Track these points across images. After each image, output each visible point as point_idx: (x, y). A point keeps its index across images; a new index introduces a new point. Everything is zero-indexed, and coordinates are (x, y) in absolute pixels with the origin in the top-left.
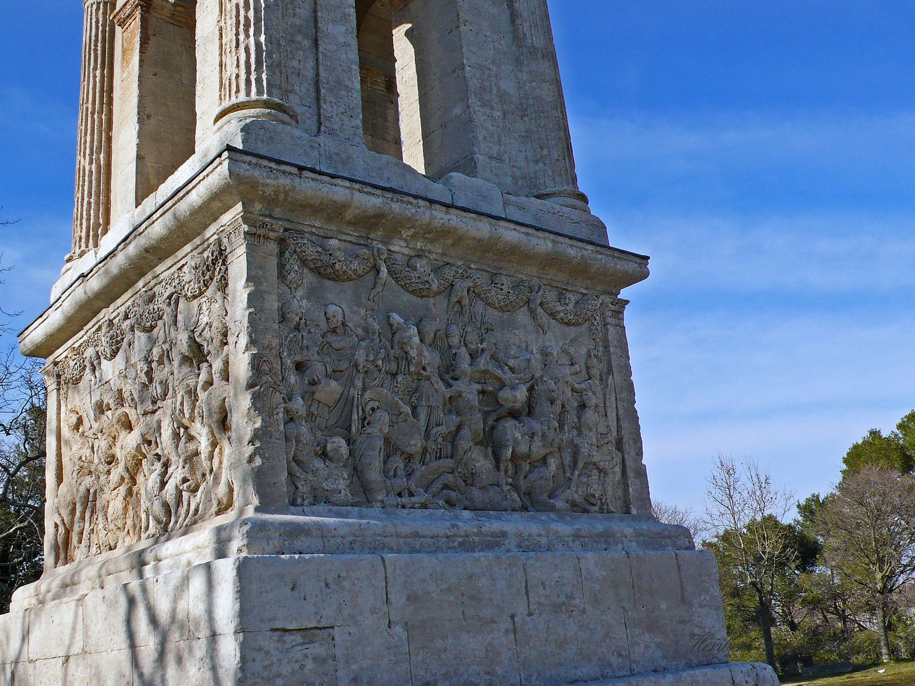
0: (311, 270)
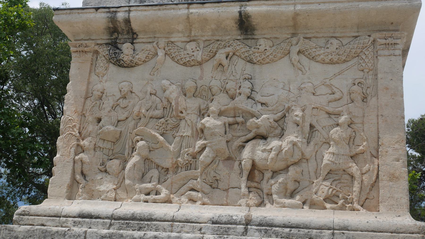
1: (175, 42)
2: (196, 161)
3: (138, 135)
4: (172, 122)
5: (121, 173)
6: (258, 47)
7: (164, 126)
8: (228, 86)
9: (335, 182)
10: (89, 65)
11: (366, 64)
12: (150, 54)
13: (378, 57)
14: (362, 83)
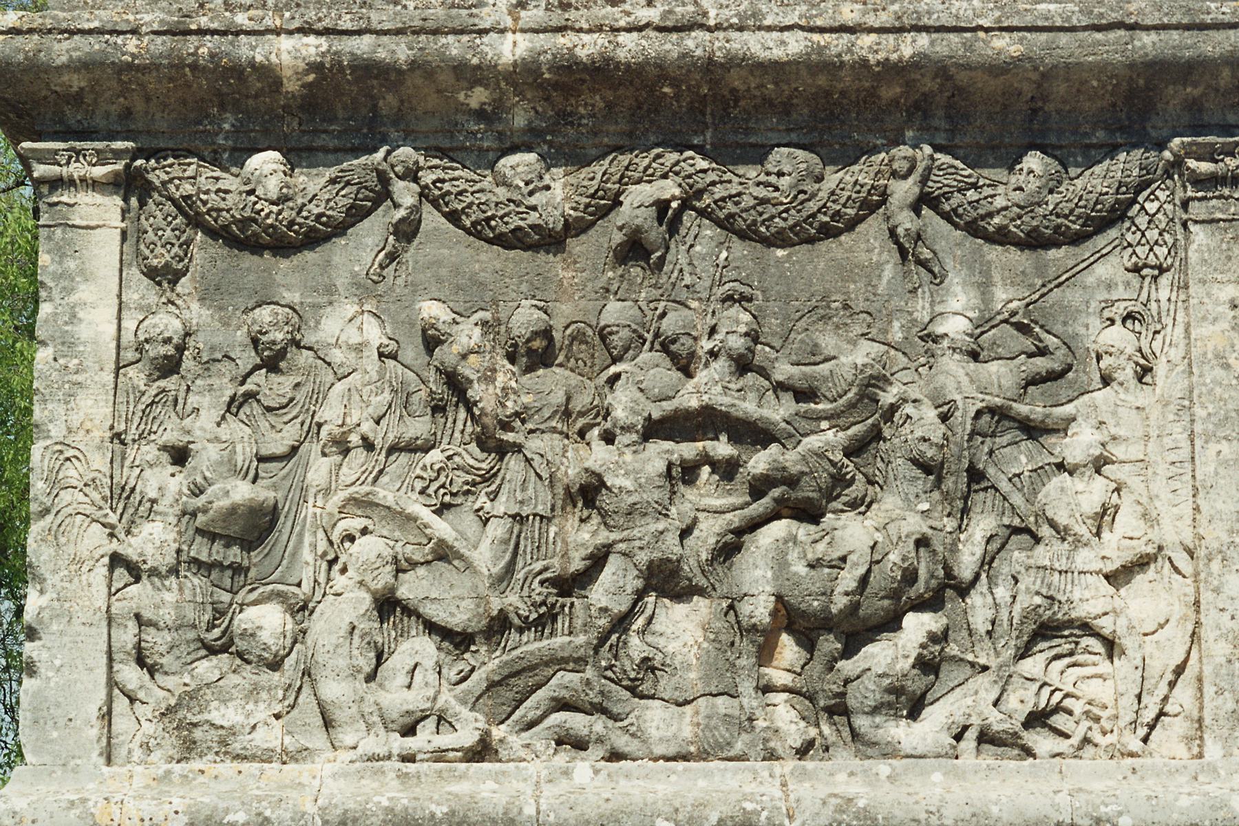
2: (572, 604)
4: (472, 462)
5: (293, 655)
7: (442, 479)
11: (1151, 250)
12: (360, 196)
14: (1138, 316)
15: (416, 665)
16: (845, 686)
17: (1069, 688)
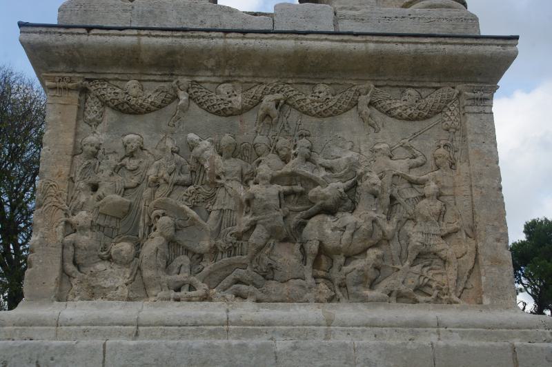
0: (113, 108)
1: (201, 82)
3: (156, 208)
5: (134, 261)
6: (317, 94)
7: (194, 196)
8: (279, 144)
9: (426, 269)
10: (75, 108)
13: (467, 115)
15: (182, 265)
16: (345, 275)
17: (430, 277)
